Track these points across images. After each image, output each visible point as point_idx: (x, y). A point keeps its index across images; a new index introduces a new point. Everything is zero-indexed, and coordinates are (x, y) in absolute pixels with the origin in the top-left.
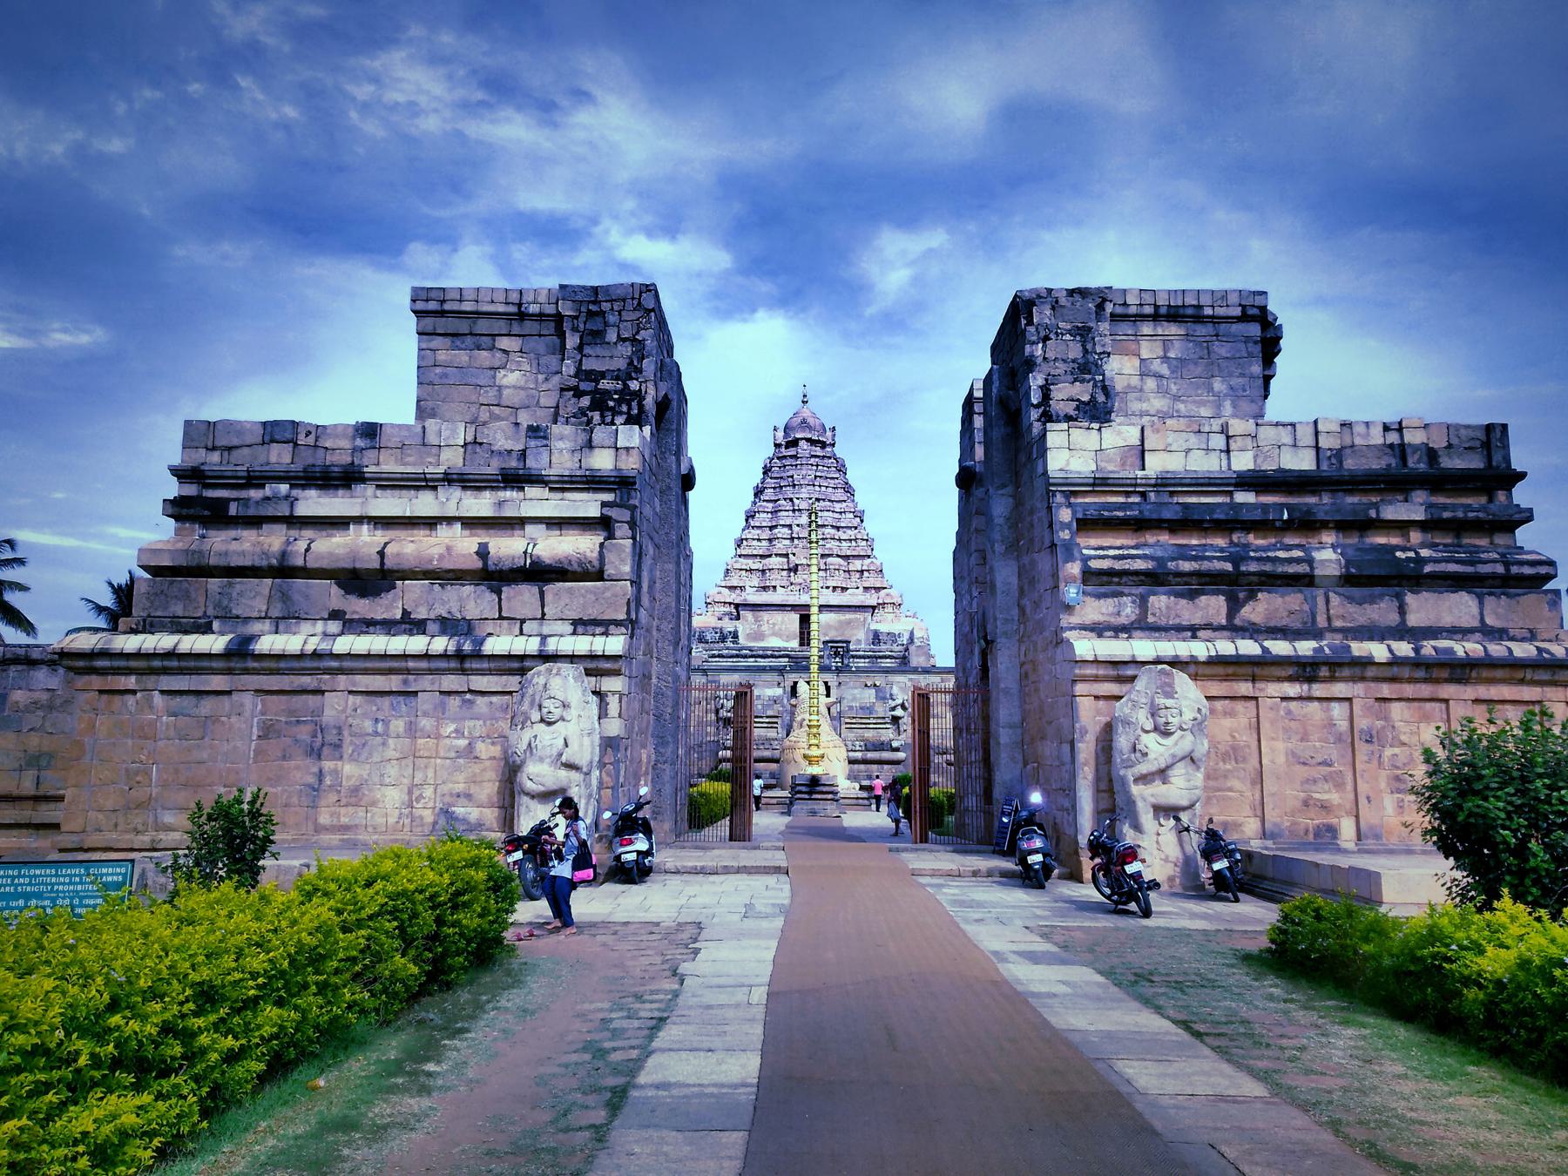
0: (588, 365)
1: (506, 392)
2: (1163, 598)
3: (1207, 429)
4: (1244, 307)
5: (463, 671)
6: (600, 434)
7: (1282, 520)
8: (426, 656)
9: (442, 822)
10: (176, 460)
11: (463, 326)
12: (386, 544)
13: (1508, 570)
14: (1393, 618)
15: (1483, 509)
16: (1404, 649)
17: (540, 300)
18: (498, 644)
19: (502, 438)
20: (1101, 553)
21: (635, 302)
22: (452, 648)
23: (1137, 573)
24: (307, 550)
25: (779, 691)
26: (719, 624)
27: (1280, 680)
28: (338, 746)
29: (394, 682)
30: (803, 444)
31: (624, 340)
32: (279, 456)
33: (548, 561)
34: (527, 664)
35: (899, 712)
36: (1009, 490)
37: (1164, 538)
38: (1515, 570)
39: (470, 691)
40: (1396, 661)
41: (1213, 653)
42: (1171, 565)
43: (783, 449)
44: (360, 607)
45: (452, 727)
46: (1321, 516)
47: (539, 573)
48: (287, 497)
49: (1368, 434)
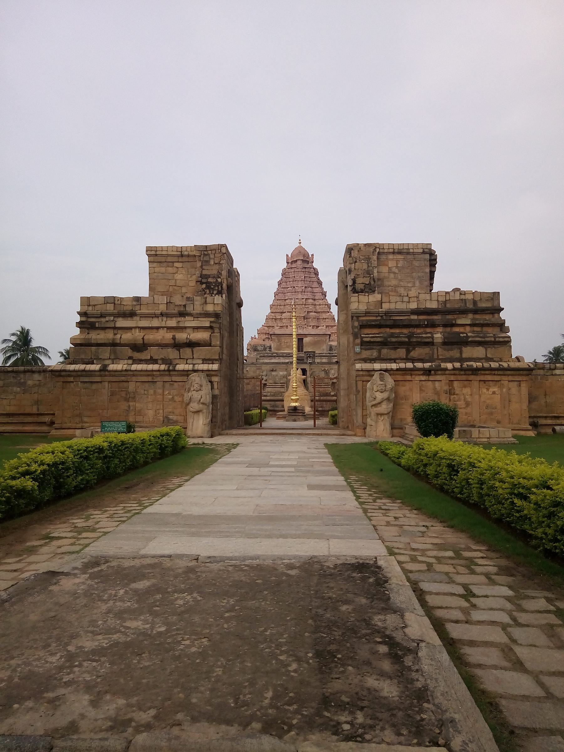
0: (205, 272)
1: (178, 282)
2: (386, 350)
3: (403, 295)
5: (170, 375)
6: (209, 299)
7: (425, 324)
8: (159, 371)
9: (166, 420)
11: (163, 259)
12: (144, 335)
13: (495, 339)
14: (458, 355)
15: (489, 320)
16: (457, 365)
17: (188, 250)
18: (180, 367)
19: (178, 300)
20: (367, 336)
21: (219, 251)
22: (166, 368)
23: (378, 342)
24: (121, 338)
25: (285, 373)
26: (263, 343)
27: (419, 375)
28: (134, 398)
29: (150, 379)
30: (299, 263)
31: (216, 264)
33: (194, 341)
34: (189, 372)
35: (335, 381)
36: (345, 312)
37: (388, 330)
38: (497, 339)
39: (172, 381)
40: (454, 369)
41: (398, 368)
42: (389, 339)
43: (290, 264)
44: (137, 355)
46: (437, 323)
47: (191, 345)
49: (455, 296)
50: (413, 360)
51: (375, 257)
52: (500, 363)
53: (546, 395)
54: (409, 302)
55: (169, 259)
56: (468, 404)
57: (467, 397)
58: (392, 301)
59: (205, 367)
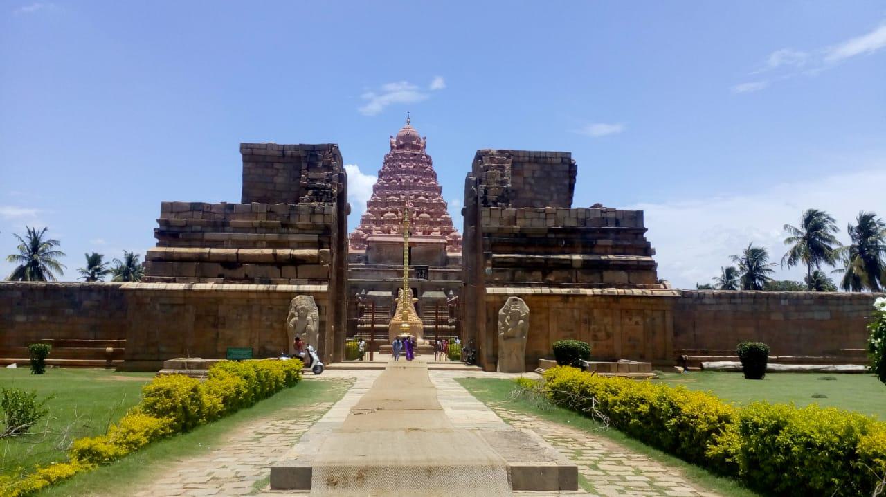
4: (562, 158)
8: (256, 292)
10: (159, 217)
18: (282, 287)
22: (265, 289)
25: (389, 294)
28: (224, 324)
32: (198, 217)
38: (640, 263)
40: (594, 296)
44: (229, 273)
45: (264, 318)
47: (295, 261)
48: (201, 231)
50: (550, 285)
51: (507, 166)
52: (644, 290)
53: (694, 327)
54: (546, 219)
55: (268, 159)
56: (609, 336)
57: (608, 327)
58: (527, 217)
59: (312, 288)
